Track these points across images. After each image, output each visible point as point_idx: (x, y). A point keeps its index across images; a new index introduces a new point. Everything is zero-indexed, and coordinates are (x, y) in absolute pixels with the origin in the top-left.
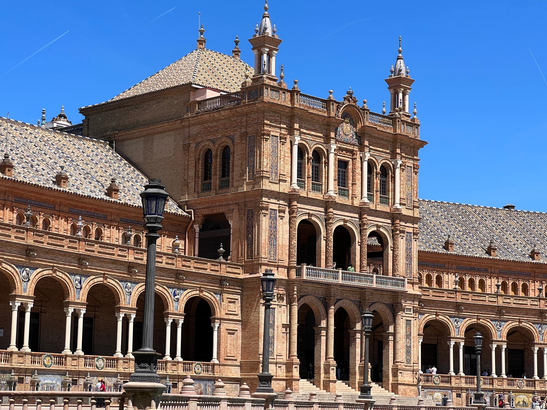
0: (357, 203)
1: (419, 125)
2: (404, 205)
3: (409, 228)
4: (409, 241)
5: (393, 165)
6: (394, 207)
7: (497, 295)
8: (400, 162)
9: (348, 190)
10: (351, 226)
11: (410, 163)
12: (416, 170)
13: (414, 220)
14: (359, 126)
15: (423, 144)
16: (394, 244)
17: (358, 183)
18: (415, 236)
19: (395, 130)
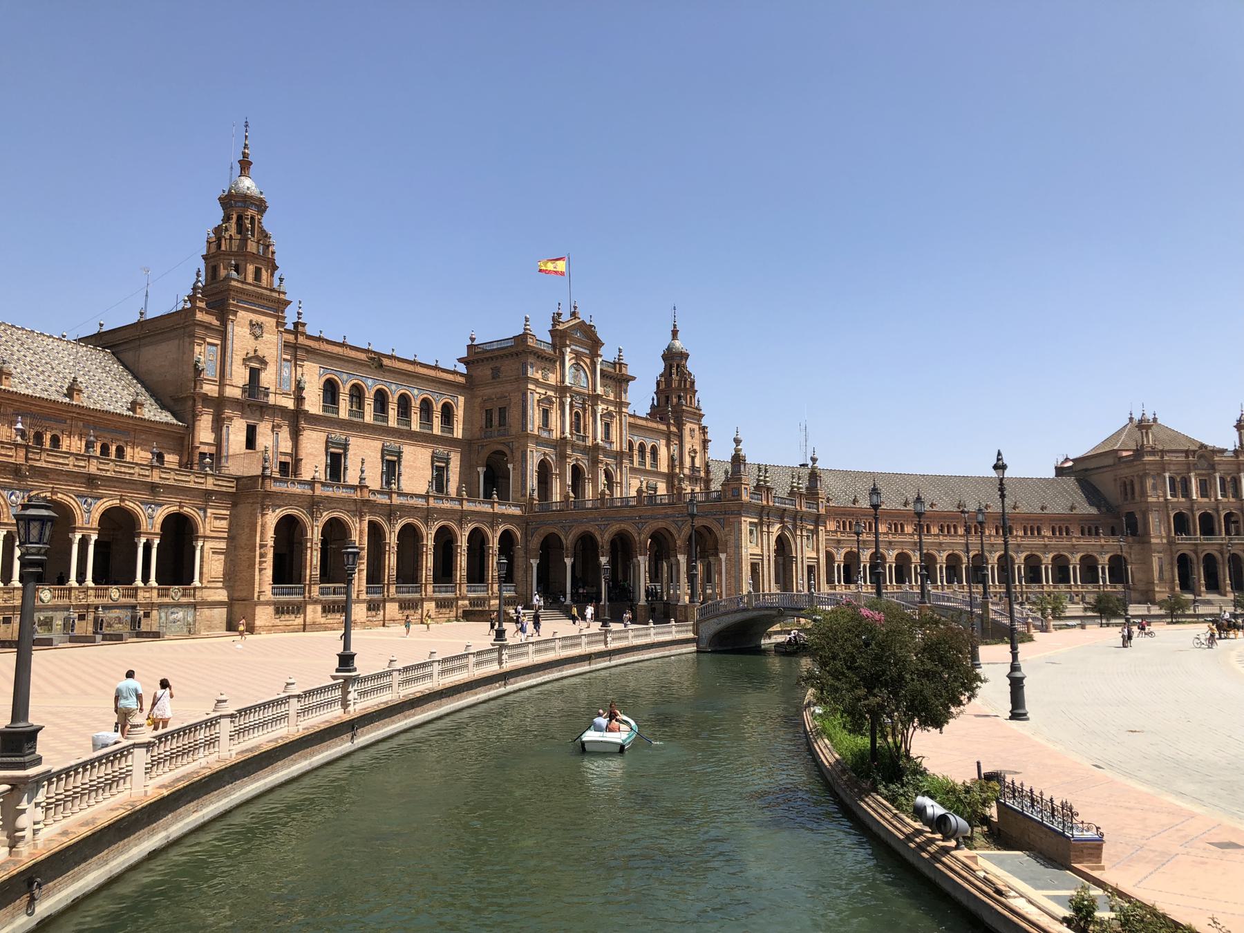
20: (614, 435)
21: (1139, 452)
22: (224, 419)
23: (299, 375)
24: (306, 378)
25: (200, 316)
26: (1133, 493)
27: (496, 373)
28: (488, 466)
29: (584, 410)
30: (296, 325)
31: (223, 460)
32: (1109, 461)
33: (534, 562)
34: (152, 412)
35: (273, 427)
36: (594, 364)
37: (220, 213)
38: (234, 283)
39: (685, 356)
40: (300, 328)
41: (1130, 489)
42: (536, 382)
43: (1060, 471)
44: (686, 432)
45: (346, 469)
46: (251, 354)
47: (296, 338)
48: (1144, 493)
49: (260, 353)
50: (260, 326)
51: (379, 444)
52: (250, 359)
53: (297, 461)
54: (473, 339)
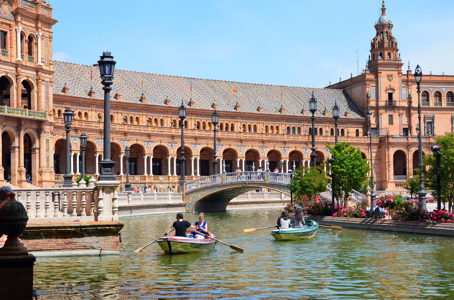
0: (13, 61)
1: (52, 9)
2: (44, 62)
3: (46, 77)
4: (47, 87)
5: (37, 36)
6: (37, 64)
7: (148, 126)
8: (41, 34)
9: (7, 52)
10: (11, 77)
11: (47, 34)
12: (50, 39)
13: (50, 73)
14: (14, 7)
15: (55, 21)
16: (38, 89)
17: (14, 47)
18: (51, 84)
19: (37, 11)
22: (379, 115)
23: (409, 92)
24: (411, 94)
25: (368, 77)
30: (408, 71)
31: (380, 130)
34: (353, 115)
35: (399, 115)
37: (375, 32)
38: (380, 61)
40: (409, 73)
46: (388, 88)
47: (408, 77)
49: (392, 87)
50: (391, 76)
52: (388, 90)
53: (410, 127)
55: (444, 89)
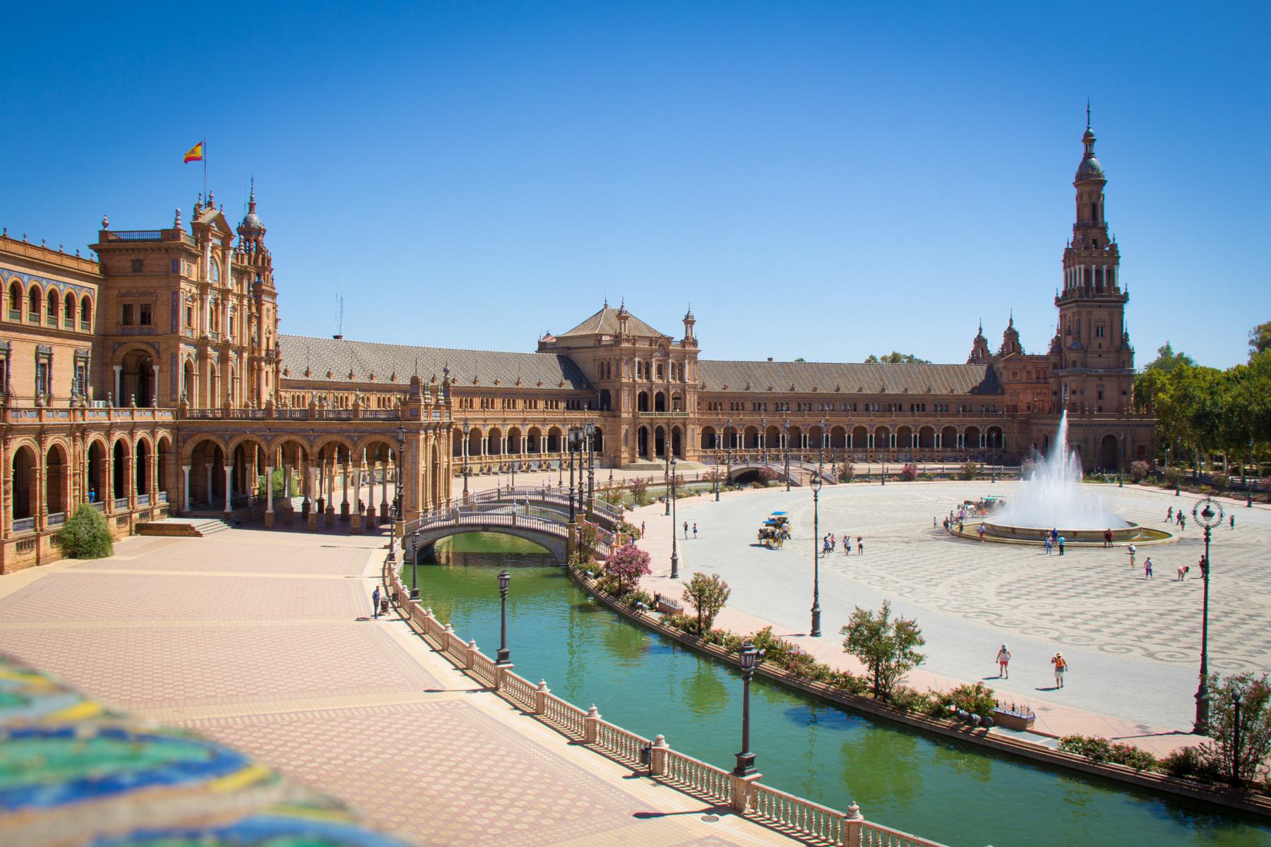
20: (236, 331)
21: (617, 338)
26: (609, 373)
27: (138, 267)
28: (124, 364)
29: (217, 305)
32: (591, 343)
33: (186, 469)
36: (224, 256)
39: (260, 231)
41: (606, 370)
42: (186, 279)
43: (543, 347)
44: (264, 313)
45: (8, 376)
48: (619, 375)
51: (33, 347)
54: (105, 225)
55: (26, 279)
